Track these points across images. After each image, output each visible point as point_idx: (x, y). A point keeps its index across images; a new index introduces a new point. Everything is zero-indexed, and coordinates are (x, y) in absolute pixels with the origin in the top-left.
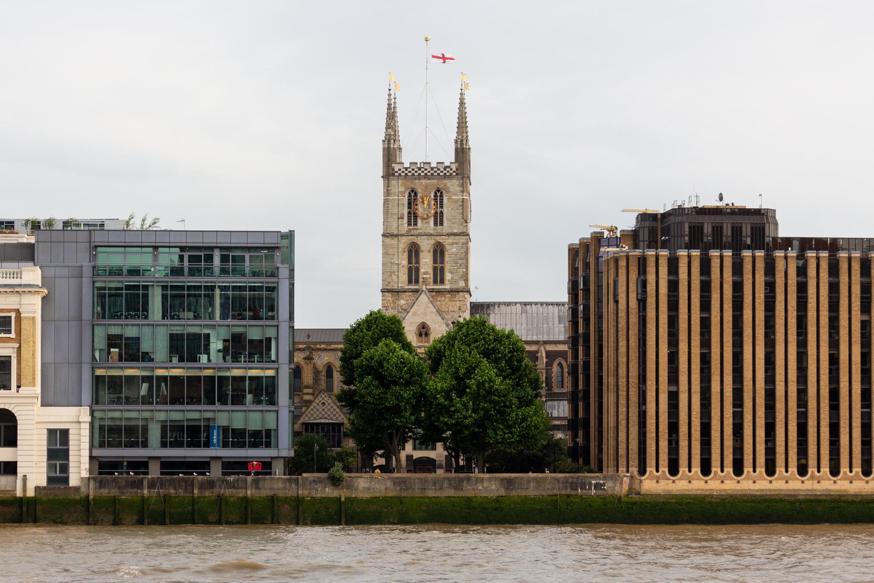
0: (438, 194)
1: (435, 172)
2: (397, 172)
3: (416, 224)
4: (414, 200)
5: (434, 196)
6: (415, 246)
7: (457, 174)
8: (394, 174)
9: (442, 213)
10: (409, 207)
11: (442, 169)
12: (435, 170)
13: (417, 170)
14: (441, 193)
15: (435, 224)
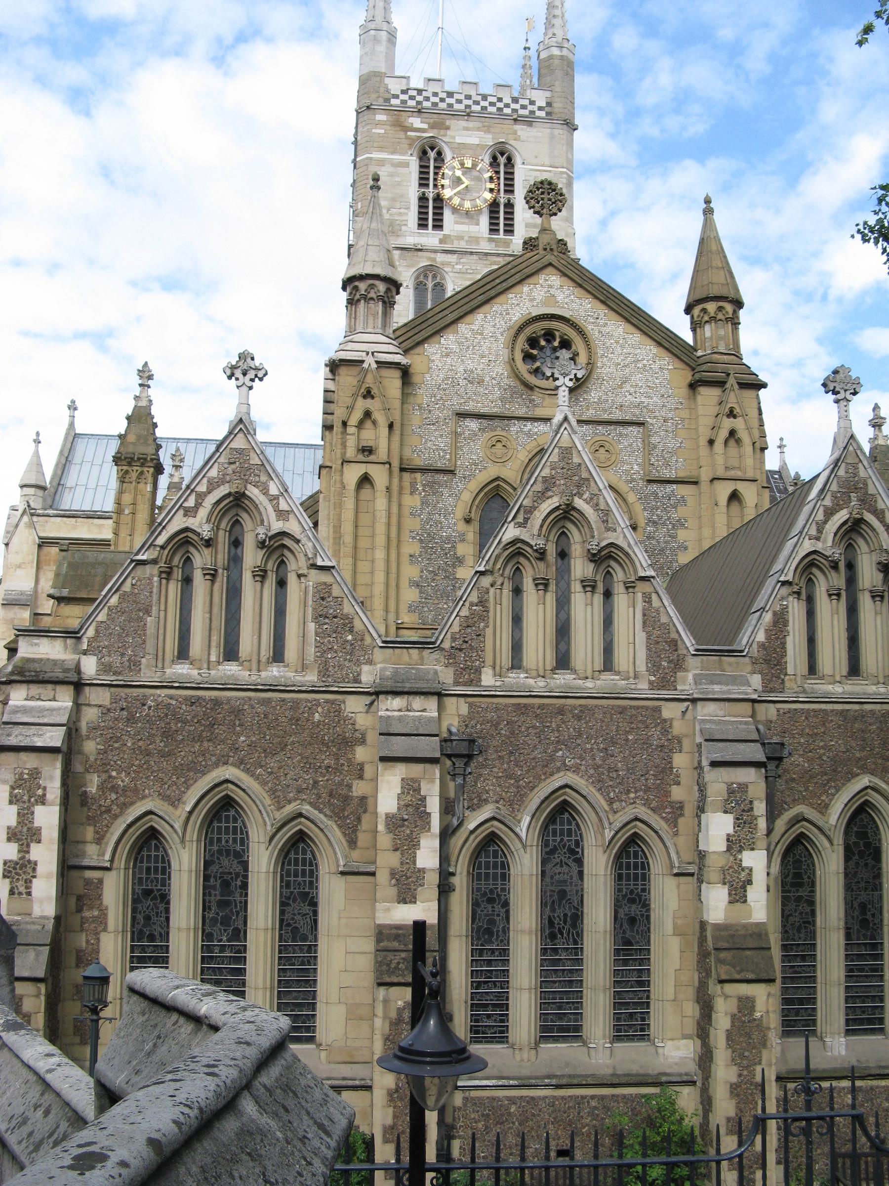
0: (502, 160)
1: (492, 104)
2: (396, 97)
3: (438, 226)
4: (435, 167)
5: (491, 165)
6: (434, 277)
7: (548, 114)
8: (387, 100)
9: (509, 205)
10: (423, 182)
11: (507, 100)
12: (490, 99)
13: (444, 95)
14: (509, 159)
15: (493, 229)
